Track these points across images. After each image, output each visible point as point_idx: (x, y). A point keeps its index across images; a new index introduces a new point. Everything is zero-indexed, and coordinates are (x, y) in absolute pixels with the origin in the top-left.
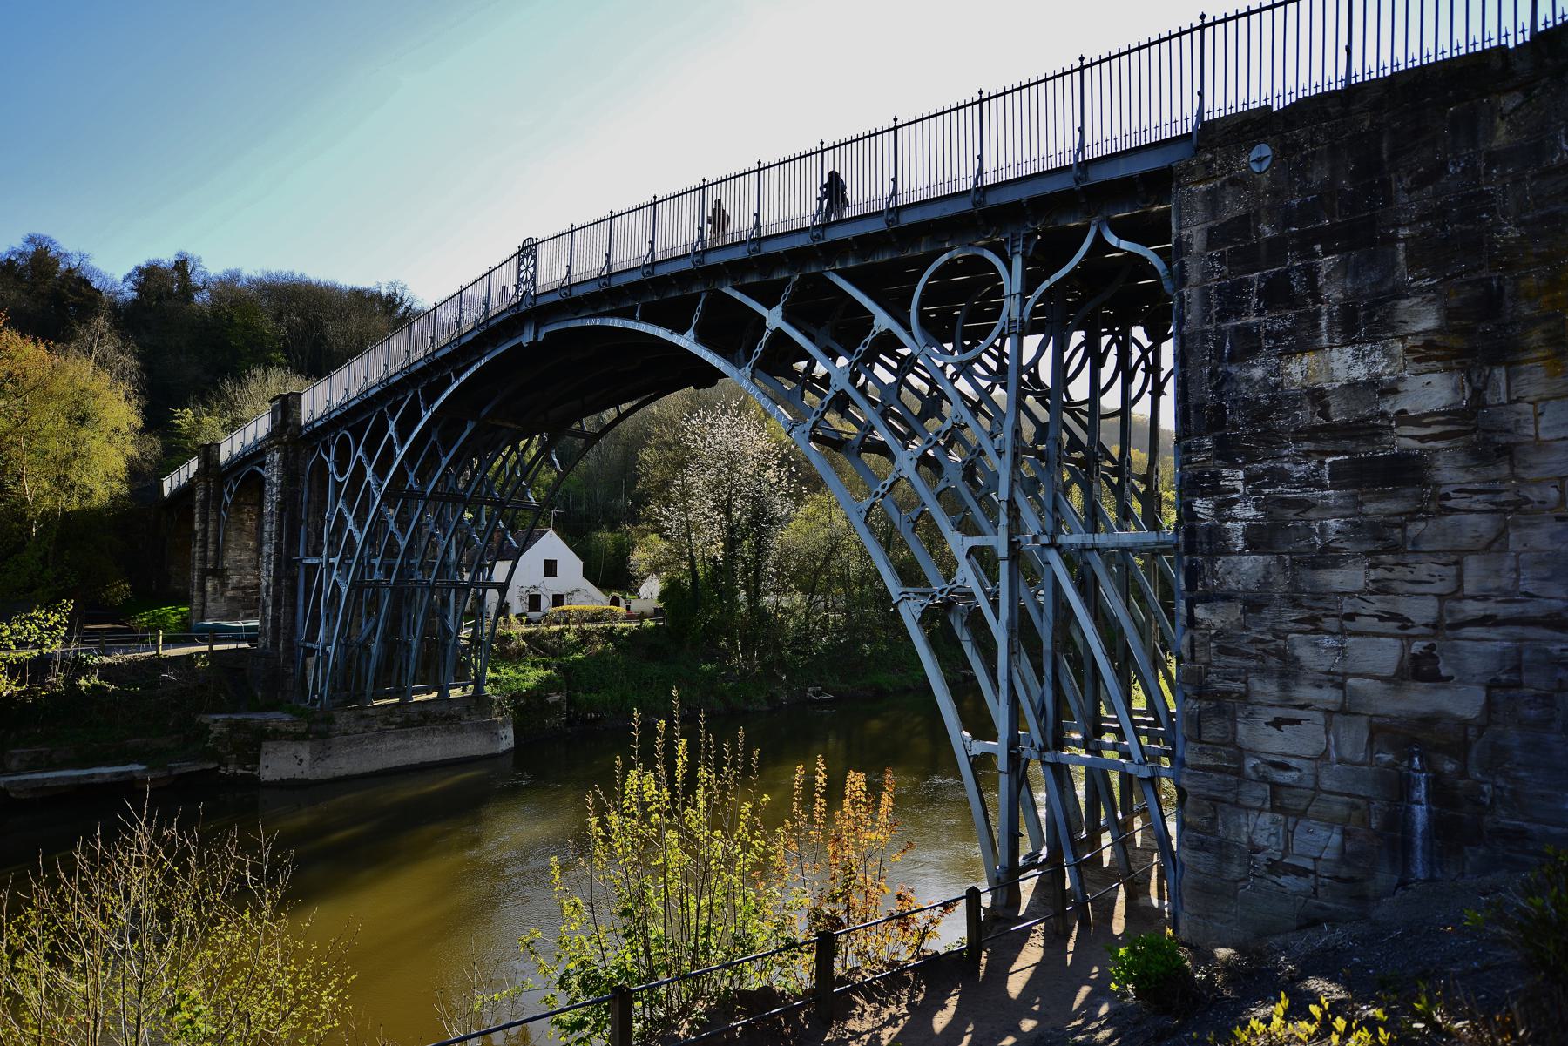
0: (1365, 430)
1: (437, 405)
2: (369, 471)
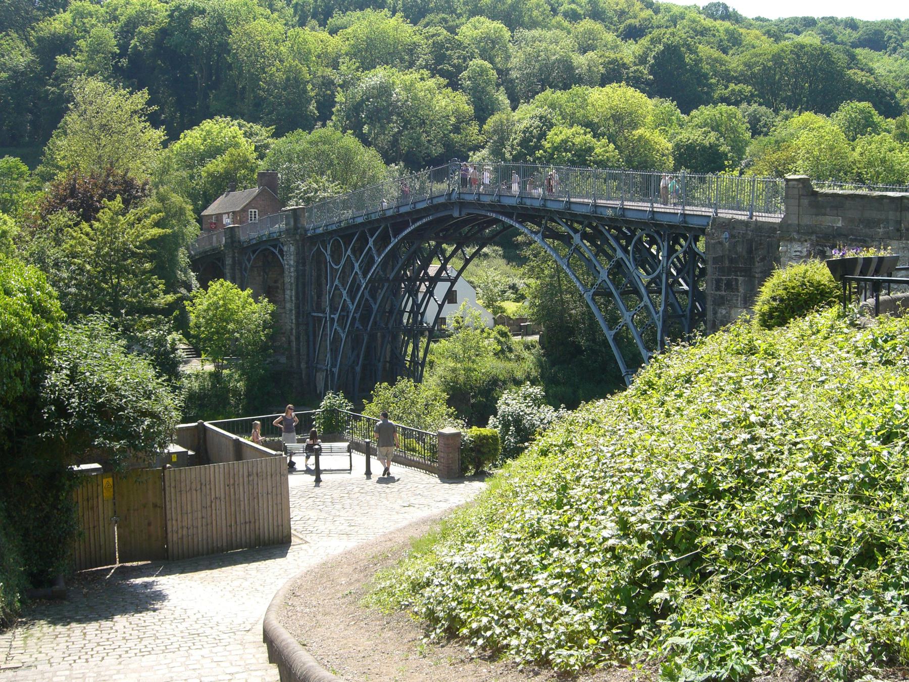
1: (401, 236)
2: (357, 265)
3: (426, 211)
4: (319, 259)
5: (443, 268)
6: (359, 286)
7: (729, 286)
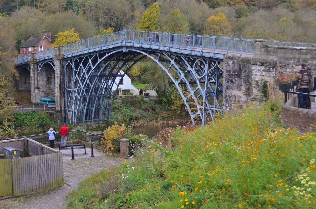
0: (239, 101)
2: (84, 70)
3: (113, 49)
4: (69, 66)
5: (119, 71)
6: (85, 78)
7: (232, 81)
